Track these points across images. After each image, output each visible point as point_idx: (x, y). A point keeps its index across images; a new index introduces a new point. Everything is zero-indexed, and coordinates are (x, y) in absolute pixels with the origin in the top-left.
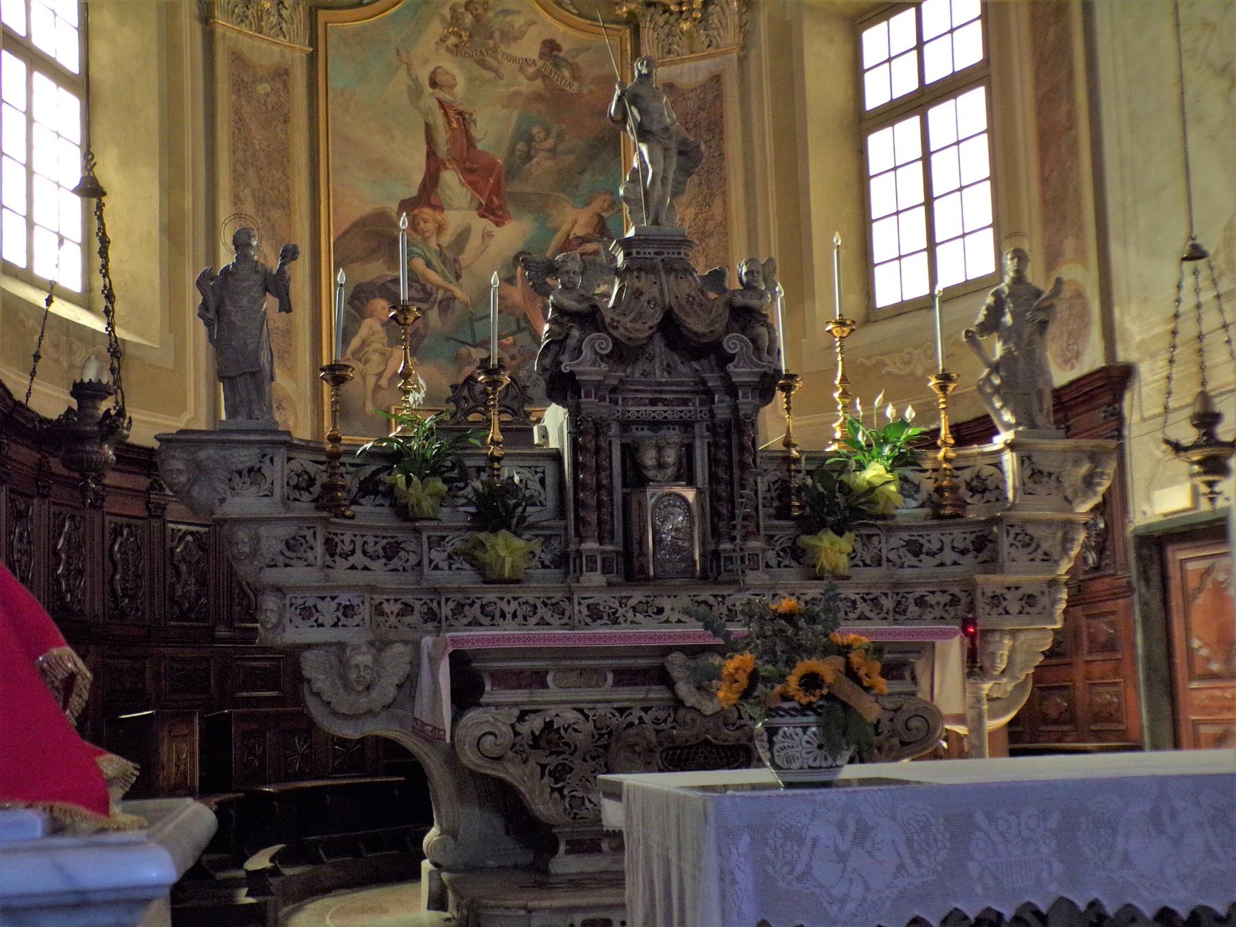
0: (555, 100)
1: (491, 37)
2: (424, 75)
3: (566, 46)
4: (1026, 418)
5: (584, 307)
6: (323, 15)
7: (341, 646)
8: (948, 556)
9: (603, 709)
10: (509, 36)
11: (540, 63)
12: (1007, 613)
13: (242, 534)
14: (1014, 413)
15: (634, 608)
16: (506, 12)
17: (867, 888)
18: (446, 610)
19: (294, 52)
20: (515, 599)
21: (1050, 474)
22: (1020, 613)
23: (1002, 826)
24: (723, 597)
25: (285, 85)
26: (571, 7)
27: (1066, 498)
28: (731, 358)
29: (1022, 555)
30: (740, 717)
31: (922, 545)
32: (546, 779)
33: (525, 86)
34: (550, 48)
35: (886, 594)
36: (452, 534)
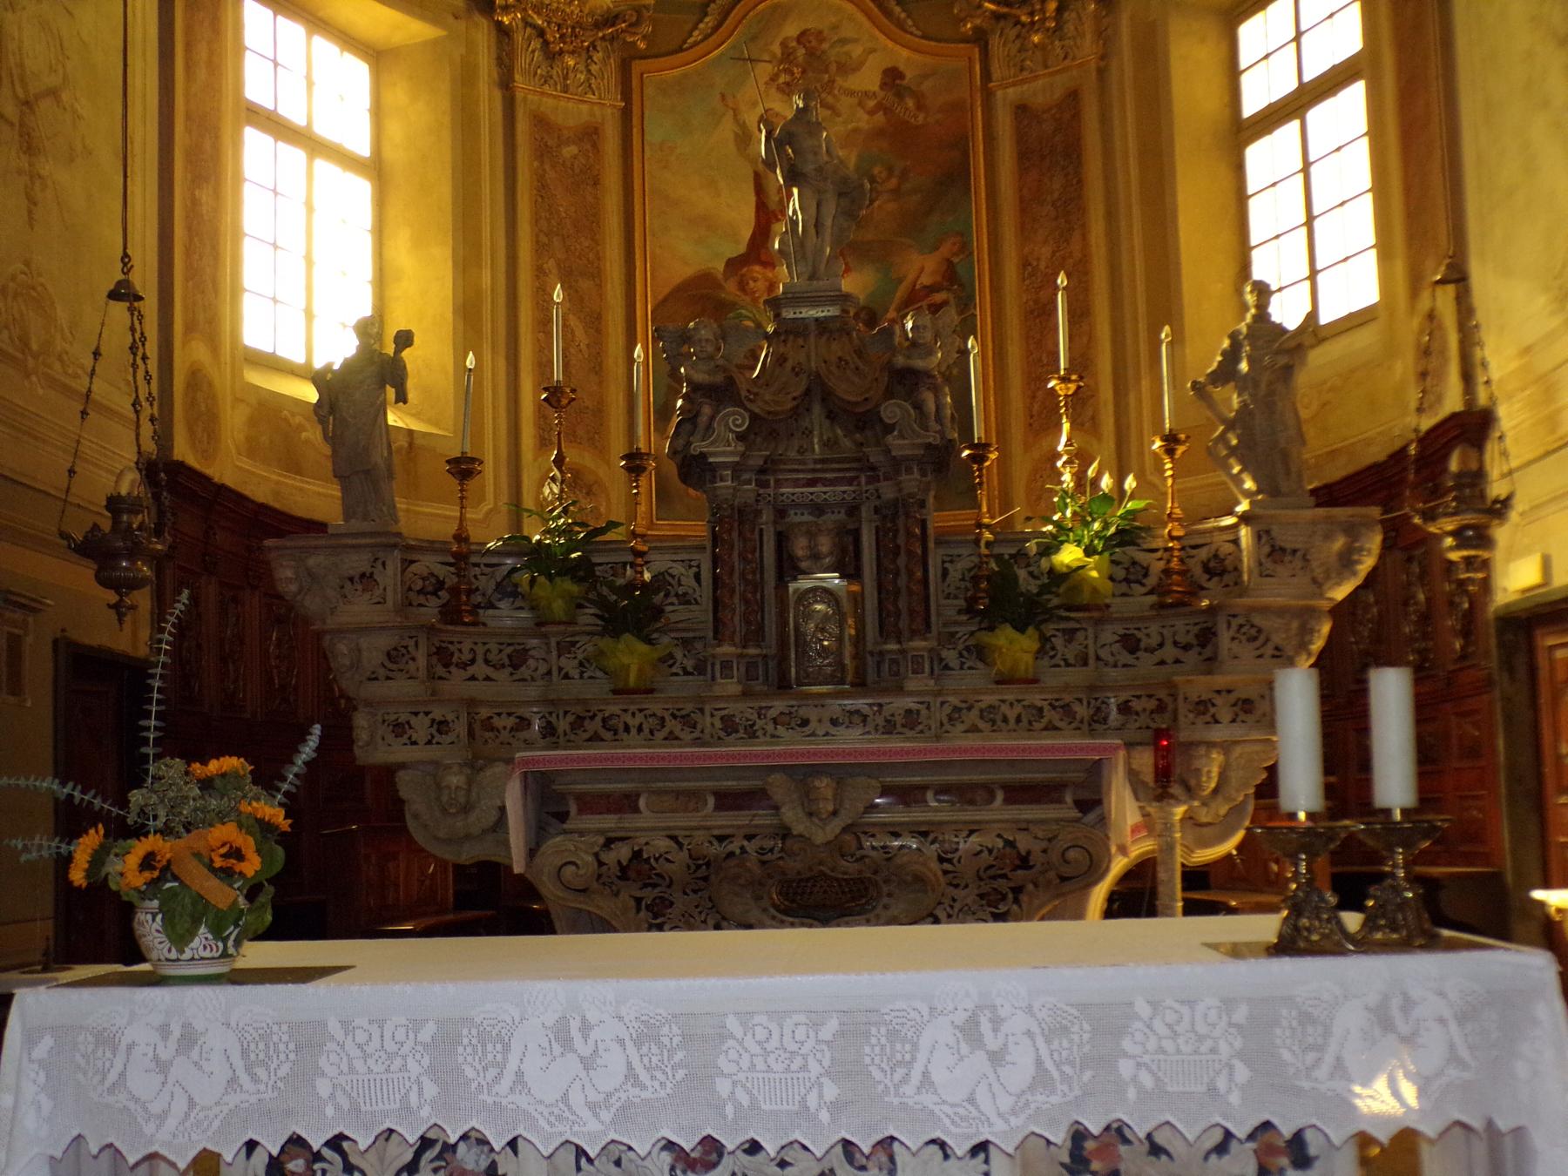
1: (827, 72)
2: (751, 118)
3: (909, 74)
4: (1269, 487)
5: (719, 378)
6: (637, 66)
7: (436, 763)
8: (1169, 652)
9: (700, 836)
10: (845, 68)
11: (882, 94)
12: (1217, 722)
13: (342, 647)
14: (1255, 479)
15: (775, 721)
16: (843, 41)
17: (192, 1103)
18: (563, 725)
19: (601, 107)
20: (641, 711)
21: (1294, 551)
22: (1233, 721)
23: (361, 1037)
24: (880, 705)
25: (594, 146)
26: (913, 29)
27: (1314, 581)
28: (889, 429)
29: (1246, 651)
30: (861, 848)
31: (1139, 640)
32: (643, 914)
33: (863, 121)
34: (892, 77)
35: (1080, 700)
36: (585, 638)
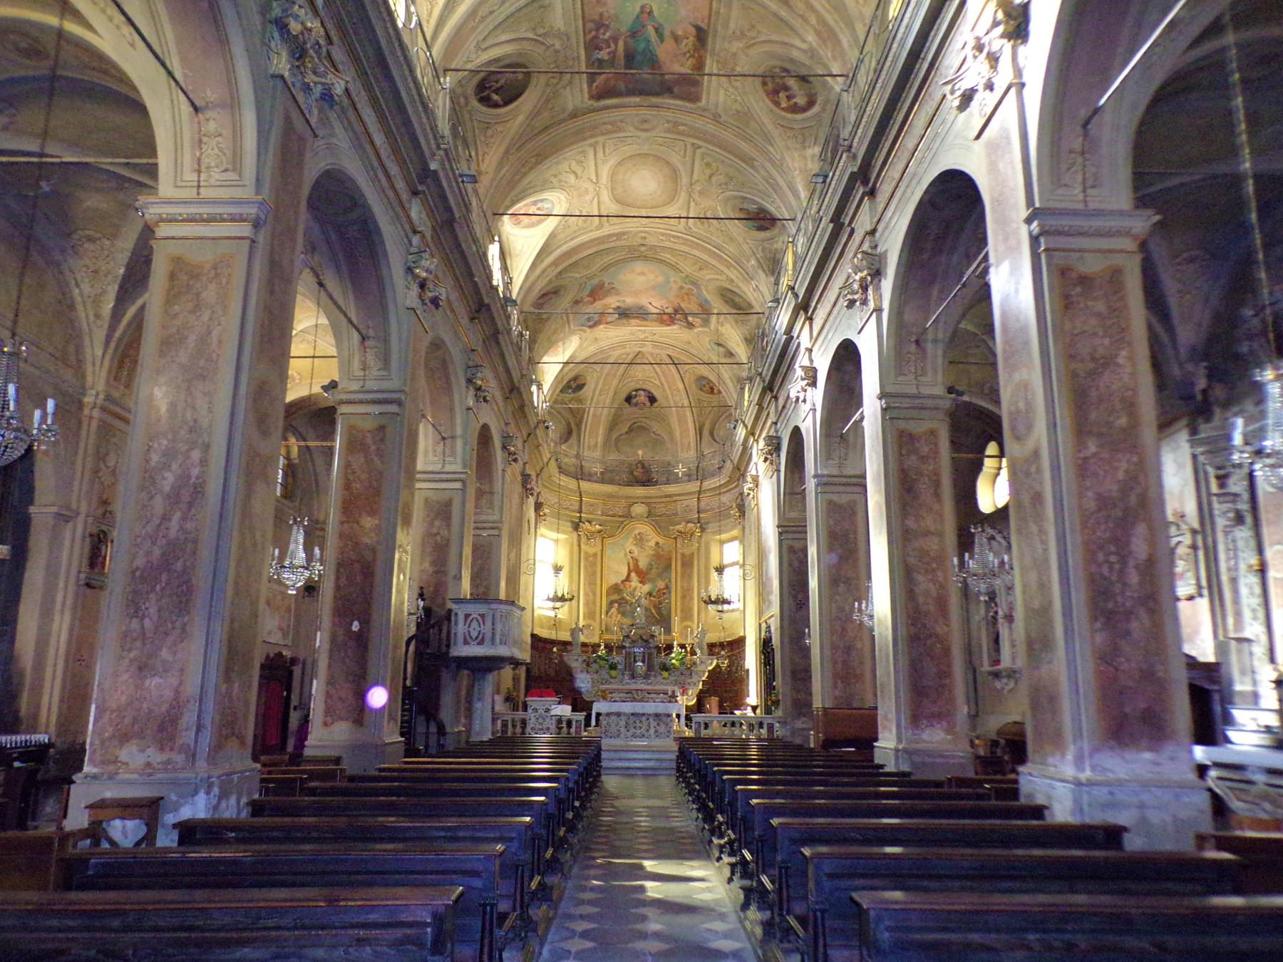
0: (657, 556)
19: (598, 549)
34: (657, 543)
